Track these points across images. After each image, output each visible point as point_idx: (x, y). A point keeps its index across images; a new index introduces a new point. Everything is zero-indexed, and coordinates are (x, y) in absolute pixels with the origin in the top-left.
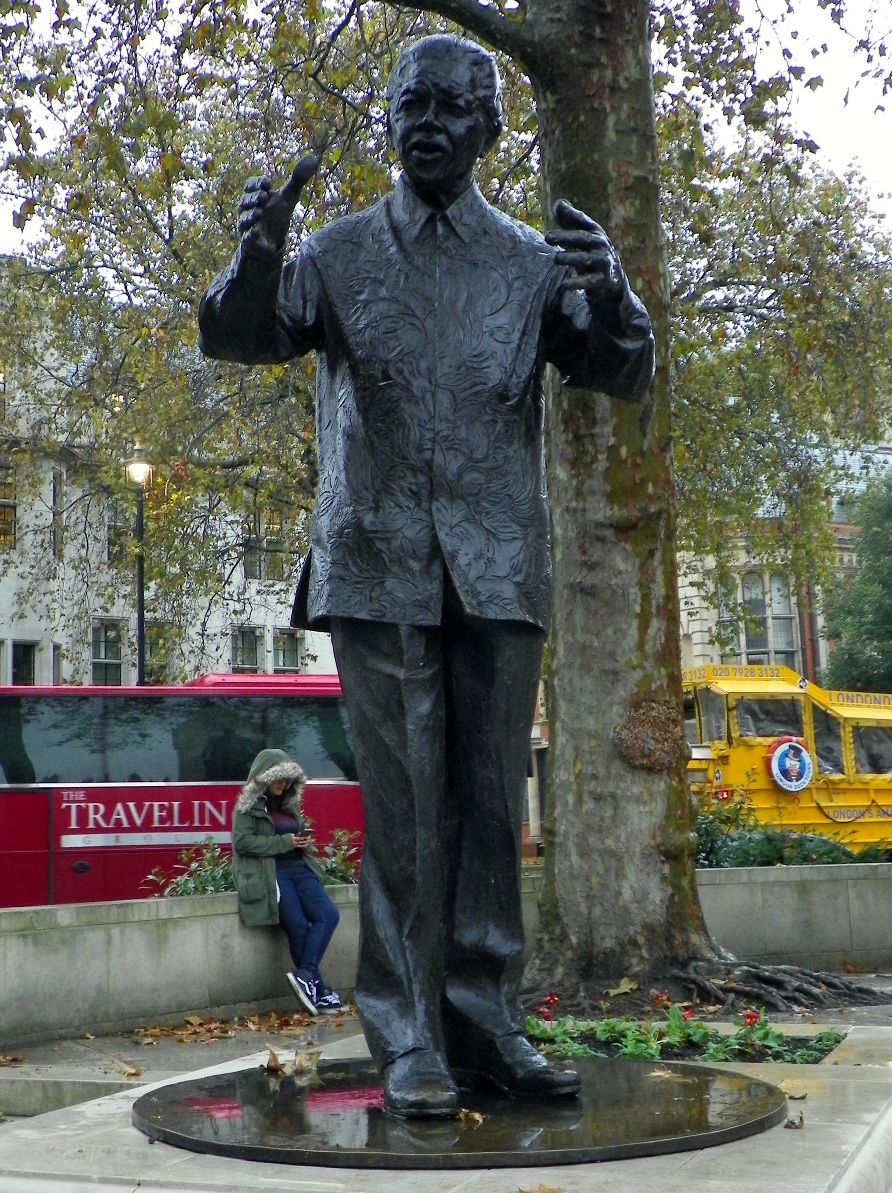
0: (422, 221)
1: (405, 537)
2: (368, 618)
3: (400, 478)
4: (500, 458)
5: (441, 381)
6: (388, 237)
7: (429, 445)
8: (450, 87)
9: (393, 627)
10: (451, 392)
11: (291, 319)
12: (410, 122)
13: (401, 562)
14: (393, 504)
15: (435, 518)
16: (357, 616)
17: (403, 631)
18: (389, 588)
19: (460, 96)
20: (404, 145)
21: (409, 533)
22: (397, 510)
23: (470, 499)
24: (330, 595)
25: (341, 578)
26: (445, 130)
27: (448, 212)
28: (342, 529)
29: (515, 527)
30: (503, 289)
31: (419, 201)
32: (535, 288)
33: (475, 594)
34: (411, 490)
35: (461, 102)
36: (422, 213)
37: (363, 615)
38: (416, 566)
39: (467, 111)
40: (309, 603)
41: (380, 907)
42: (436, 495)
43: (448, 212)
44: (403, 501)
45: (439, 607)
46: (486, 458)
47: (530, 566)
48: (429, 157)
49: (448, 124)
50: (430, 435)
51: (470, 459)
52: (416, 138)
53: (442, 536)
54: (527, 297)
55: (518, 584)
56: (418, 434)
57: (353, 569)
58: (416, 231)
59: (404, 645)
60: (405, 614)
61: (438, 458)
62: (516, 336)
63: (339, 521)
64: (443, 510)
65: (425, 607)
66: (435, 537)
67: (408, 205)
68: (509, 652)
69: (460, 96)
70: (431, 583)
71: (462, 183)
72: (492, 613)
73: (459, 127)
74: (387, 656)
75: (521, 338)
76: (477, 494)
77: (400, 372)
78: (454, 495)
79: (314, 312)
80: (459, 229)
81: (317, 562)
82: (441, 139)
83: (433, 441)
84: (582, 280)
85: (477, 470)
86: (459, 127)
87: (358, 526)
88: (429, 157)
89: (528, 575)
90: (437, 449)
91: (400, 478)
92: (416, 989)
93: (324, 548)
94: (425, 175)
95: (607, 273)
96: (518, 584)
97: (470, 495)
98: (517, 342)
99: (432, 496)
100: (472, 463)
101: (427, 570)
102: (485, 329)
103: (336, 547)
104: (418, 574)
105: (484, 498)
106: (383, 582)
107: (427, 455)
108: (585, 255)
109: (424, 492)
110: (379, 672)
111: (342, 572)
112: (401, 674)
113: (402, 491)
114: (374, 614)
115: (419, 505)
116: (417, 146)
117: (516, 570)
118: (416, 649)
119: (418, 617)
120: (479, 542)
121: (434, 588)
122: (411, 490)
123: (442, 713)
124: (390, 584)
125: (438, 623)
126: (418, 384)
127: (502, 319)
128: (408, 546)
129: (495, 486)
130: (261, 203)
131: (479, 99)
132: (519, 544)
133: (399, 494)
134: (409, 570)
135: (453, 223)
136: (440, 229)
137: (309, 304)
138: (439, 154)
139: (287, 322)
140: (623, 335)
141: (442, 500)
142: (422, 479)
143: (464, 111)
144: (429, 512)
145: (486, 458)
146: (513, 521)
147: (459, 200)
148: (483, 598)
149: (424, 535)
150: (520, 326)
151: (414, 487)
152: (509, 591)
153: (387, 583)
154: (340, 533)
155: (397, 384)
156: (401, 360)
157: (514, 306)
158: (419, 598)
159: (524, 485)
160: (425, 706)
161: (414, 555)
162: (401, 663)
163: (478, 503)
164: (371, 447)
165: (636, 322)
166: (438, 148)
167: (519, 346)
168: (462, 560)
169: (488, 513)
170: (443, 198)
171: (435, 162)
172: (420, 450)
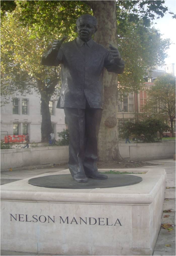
35: (91, 26)
36: (83, 43)
48: (84, 34)
63: (66, 92)
82: (87, 32)
86: (90, 30)
116: (83, 33)
138: (86, 34)
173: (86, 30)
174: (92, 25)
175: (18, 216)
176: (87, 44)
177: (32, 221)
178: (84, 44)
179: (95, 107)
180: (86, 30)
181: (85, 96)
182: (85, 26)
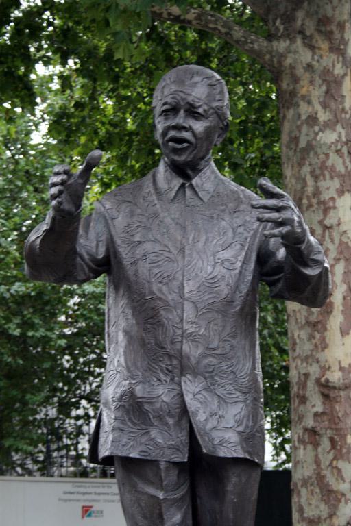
0: (176, 188)
1: (163, 401)
2: (138, 456)
3: (160, 361)
4: (228, 347)
5: (187, 295)
7: (179, 339)
8: (193, 101)
9: (154, 463)
10: (194, 303)
11: (88, 254)
14: (155, 379)
15: (183, 388)
16: (131, 455)
17: (163, 466)
18: (152, 436)
19: (200, 107)
20: (163, 139)
21: (166, 399)
22: (158, 383)
23: (207, 375)
24: (113, 442)
25: (121, 430)
26: (189, 129)
28: (122, 396)
29: (238, 394)
30: (230, 234)
31: (174, 174)
32: (252, 232)
33: (212, 440)
34: (167, 369)
35: (200, 110)
36: (177, 182)
38: (171, 421)
40: (100, 447)
42: (184, 373)
43: (194, 182)
44: (162, 376)
45: (186, 449)
46: (217, 348)
47: (248, 420)
48: (179, 146)
49: (191, 124)
50: (179, 332)
52: (172, 133)
53: (188, 399)
54: (246, 239)
55: (239, 433)
56: (172, 331)
57: (129, 424)
59: (163, 475)
60: (163, 454)
61: (186, 348)
62: (239, 264)
63: (120, 391)
64: (188, 383)
66: (183, 402)
67: (167, 178)
68: (234, 479)
69: (200, 107)
70: (181, 433)
71: (203, 163)
72: (223, 453)
73: (199, 126)
74: (151, 483)
75: (242, 267)
76: (212, 372)
77: (160, 290)
78: (195, 374)
81: (105, 418)
83: (182, 336)
84: (276, 231)
85: (212, 355)
86: (199, 126)
87: (131, 393)
88: (179, 146)
89: (247, 427)
90: (185, 341)
91: (160, 361)
93: (110, 409)
94: (176, 158)
95: (293, 227)
96: (239, 433)
97: (207, 372)
98: (239, 269)
99: (182, 374)
100: (209, 352)
101: (178, 423)
102: (217, 261)
103: (118, 408)
104: (172, 427)
105: (216, 375)
106: (149, 432)
107: (178, 346)
109: (176, 371)
110: (147, 494)
111: (121, 426)
112: (161, 495)
113: (162, 371)
114: (143, 454)
115: (172, 380)
117: (239, 423)
118: (172, 477)
119: (173, 457)
121: (183, 436)
122: (167, 369)
124: (154, 433)
125: (186, 460)
126: (172, 297)
127: (227, 254)
129: (224, 366)
131: (212, 108)
132: (241, 405)
133: (159, 371)
135: (197, 189)
137: (101, 244)
138: (186, 145)
139: (86, 257)
140: (306, 265)
141: (188, 376)
143: (203, 116)
145: (217, 348)
146: (236, 390)
148: (216, 443)
149: (176, 400)
150: (241, 258)
151: (170, 368)
152: (233, 437)
153: (151, 433)
154: (120, 399)
155: (160, 299)
156: (160, 282)
158: (173, 443)
159: (244, 365)
162: (162, 488)
163: (212, 377)
165: (315, 257)
167: (240, 272)
169: (219, 384)
170: (190, 172)
172: (173, 343)
173: (184, 128)
174: (206, 108)
176: (191, 185)
178: (183, 186)
179: (222, 454)
180: (184, 128)
181: (184, 411)
182: (182, 112)
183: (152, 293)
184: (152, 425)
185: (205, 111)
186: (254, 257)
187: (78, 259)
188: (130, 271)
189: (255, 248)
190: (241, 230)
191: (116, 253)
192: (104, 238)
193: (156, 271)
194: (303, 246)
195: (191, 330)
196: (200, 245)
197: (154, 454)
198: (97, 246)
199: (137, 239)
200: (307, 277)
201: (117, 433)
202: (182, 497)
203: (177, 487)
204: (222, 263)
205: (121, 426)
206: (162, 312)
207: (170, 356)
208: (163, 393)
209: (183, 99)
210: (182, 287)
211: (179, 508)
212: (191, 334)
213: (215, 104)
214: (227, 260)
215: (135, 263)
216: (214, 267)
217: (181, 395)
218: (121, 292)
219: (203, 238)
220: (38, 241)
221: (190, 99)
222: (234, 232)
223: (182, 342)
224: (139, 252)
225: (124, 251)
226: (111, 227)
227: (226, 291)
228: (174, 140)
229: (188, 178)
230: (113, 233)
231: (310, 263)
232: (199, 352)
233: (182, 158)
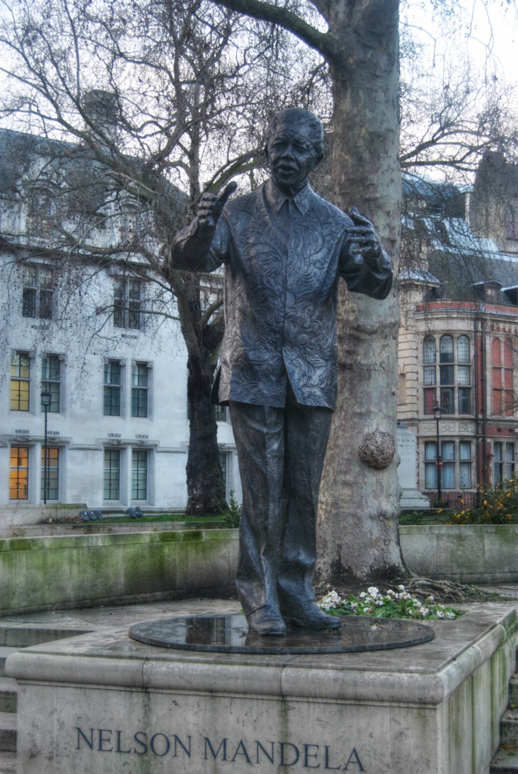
0: (282, 204)
5: (289, 287)
6: (264, 209)
7: (282, 319)
9: (260, 407)
11: (214, 250)
12: (278, 154)
13: (266, 376)
16: (244, 401)
17: (267, 410)
19: (304, 143)
24: (231, 391)
25: (237, 383)
27: (295, 200)
28: (238, 358)
29: (322, 361)
30: (320, 241)
35: (304, 146)
36: (282, 199)
37: (247, 401)
38: (273, 379)
39: (308, 150)
41: (250, 542)
44: (268, 345)
48: (287, 173)
49: (297, 156)
50: (282, 314)
51: (302, 327)
52: (281, 163)
54: (332, 245)
58: (278, 208)
62: (326, 265)
63: (236, 354)
65: (276, 398)
66: (283, 365)
69: (304, 143)
71: (302, 184)
74: (258, 422)
77: (269, 282)
79: (226, 246)
80: (300, 209)
82: (293, 165)
83: (284, 317)
84: (361, 250)
86: (302, 158)
87: (245, 357)
88: (287, 173)
89: (327, 385)
92: (266, 579)
93: (228, 366)
94: (284, 181)
99: (283, 344)
103: (235, 367)
107: (281, 324)
108: (363, 238)
110: (254, 429)
111: (237, 380)
112: (265, 430)
113: (269, 342)
115: (276, 349)
117: (322, 381)
120: (304, 367)
121: (282, 390)
123: (283, 449)
124: (261, 386)
126: (278, 288)
127: (319, 256)
128: (269, 368)
129: (313, 341)
130: (211, 208)
132: (324, 369)
134: (270, 380)
136: (291, 207)
138: (292, 172)
139: (213, 252)
140: (378, 272)
142: (278, 336)
144: (281, 352)
145: (310, 327)
147: (300, 193)
150: (328, 260)
152: (318, 392)
154: (237, 360)
155: (267, 288)
157: (325, 250)
159: (327, 340)
160: (275, 446)
161: (273, 374)
162: (265, 425)
164: (254, 320)
165: (385, 266)
166: (291, 168)
167: (327, 271)
168: (296, 376)
170: (293, 192)
171: (290, 175)
173: (292, 160)
174: (308, 143)
175: (96, 734)
176: (293, 202)
177: (133, 751)
178: (287, 202)
179: (309, 404)
180: (292, 160)
181: (283, 373)
183: (262, 284)
184: (260, 380)
185: (307, 146)
186: (337, 258)
187: (209, 256)
188: (247, 265)
189: (338, 252)
190: (328, 238)
191: (235, 251)
192: (226, 238)
193: (266, 267)
194: (378, 260)
195: (291, 313)
196: (299, 249)
197: (261, 401)
198: (221, 244)
199: (251, 241)
200: (378, 280)
201: (235, 385)
202: (279, 433)
203: (276, 424)
204: (315, 264)
205: (237, 380)
206: (270, 299)
207: (275, 332)
208: (267, 357)
209: (292, 137)
210: (285, 281)
211: (277, 440)
212: (291, 316)
213: (314, 141)
214: (318, 261)
215: (250, 259)
216: (309, 266)
217: (282, 360)
218: (238, 280)
219: (301, 245)
220: (183, 243)
221: (297, 136)
222: (324, 240)
223: (284, 322)
224: (253, 252)
225: (241, 250)
226: (232, 231)
227: (317, 285)
228: (283, 167)
229: (292, 196)
230: (233, 234)
231: (381, 270)
232: (296, 329)
233: (289, 181)
